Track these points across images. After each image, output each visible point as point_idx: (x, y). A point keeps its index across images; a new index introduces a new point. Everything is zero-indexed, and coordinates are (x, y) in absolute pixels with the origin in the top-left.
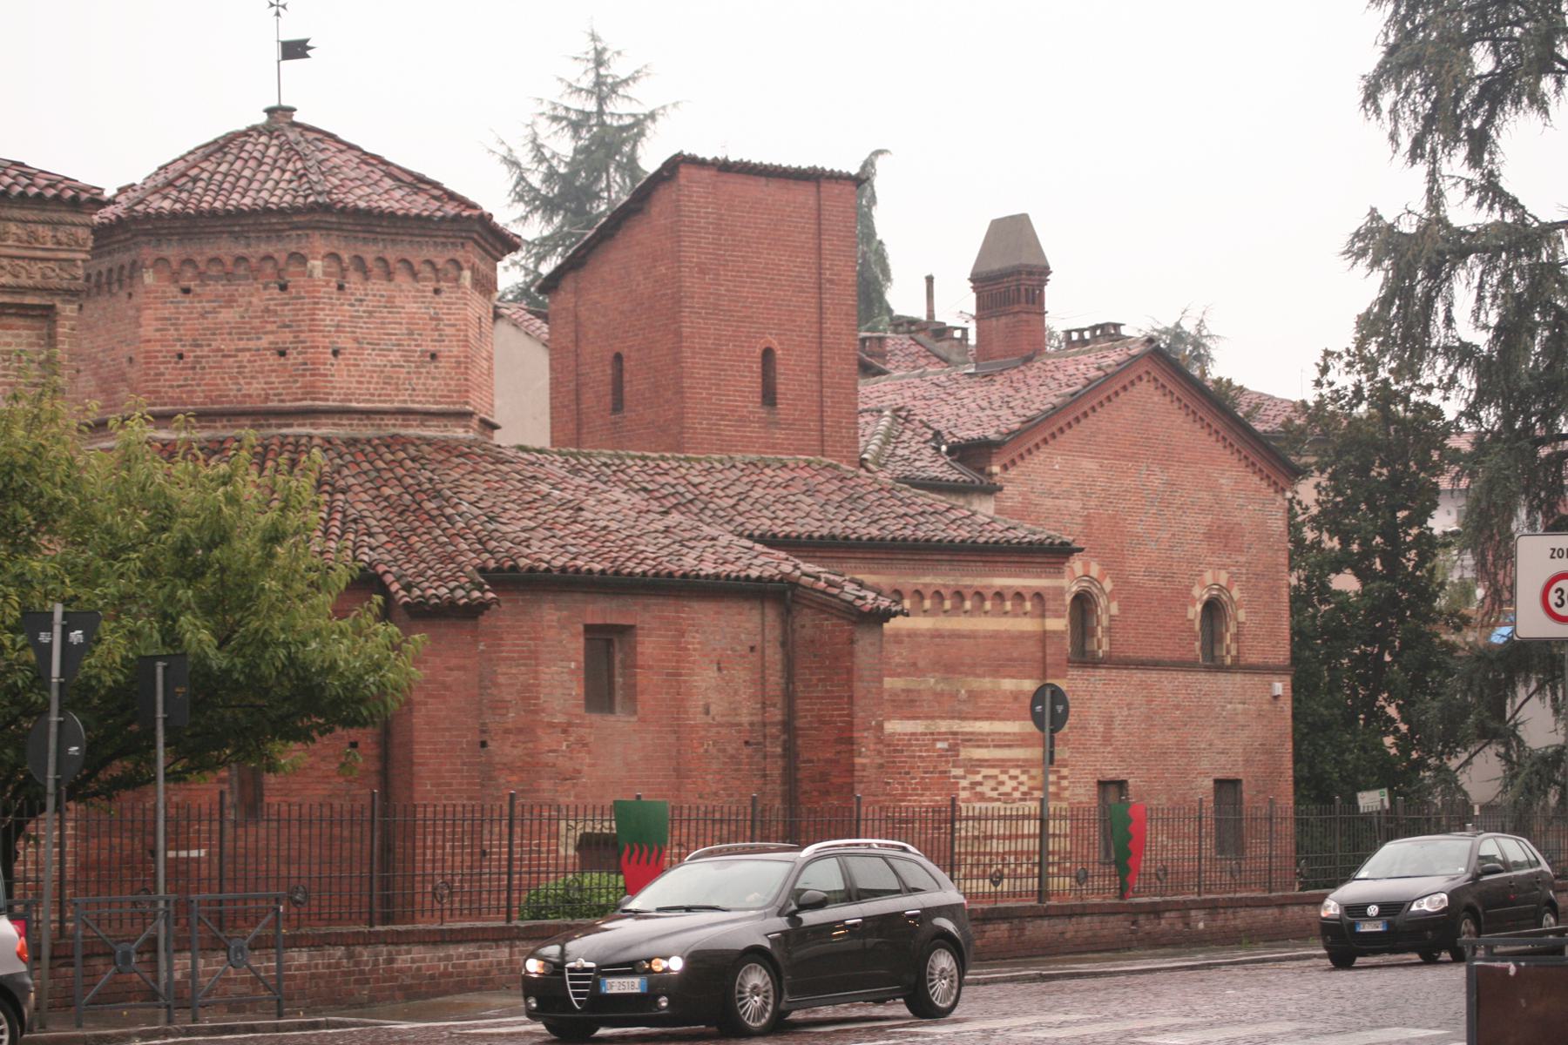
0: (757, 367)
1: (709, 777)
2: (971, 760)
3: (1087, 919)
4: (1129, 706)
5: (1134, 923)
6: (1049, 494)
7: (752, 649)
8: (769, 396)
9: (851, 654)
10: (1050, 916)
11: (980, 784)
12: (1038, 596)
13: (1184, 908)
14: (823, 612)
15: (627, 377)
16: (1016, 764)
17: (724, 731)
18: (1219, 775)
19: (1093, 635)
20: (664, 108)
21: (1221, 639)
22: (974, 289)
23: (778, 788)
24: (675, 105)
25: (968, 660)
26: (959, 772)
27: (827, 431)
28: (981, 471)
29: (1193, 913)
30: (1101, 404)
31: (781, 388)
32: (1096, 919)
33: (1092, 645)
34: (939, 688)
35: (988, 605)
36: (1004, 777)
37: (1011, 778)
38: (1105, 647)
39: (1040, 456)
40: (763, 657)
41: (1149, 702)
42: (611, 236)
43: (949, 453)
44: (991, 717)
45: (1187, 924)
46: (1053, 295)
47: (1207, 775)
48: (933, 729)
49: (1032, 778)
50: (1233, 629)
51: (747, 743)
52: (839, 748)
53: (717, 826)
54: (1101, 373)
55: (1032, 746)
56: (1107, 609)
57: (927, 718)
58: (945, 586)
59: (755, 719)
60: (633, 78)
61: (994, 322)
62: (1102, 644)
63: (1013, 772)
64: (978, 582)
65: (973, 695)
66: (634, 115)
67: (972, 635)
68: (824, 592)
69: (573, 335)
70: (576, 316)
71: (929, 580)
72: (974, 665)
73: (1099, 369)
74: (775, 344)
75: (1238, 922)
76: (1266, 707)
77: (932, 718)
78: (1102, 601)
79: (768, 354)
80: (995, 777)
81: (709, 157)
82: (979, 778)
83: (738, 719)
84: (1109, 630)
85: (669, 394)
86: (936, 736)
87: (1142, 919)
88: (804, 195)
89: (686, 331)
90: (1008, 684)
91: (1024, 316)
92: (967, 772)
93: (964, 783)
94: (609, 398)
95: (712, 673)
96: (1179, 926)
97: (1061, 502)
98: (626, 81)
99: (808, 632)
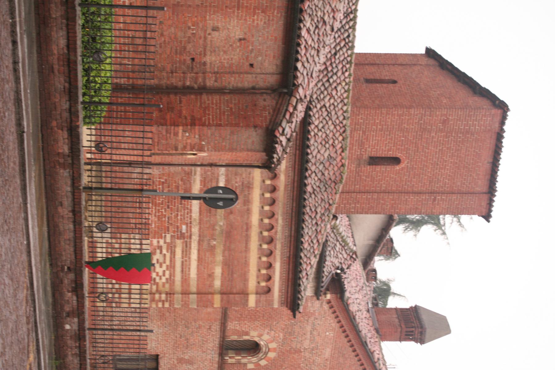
0: (391, 154)
1: (173, 29)
2: (175, 247)
3: (71, 226)
5: (69, 268)
6: (314, 329)
7: (252, 65)
8: (374, 161)
9: (247, 126)
10: (73, 193)
11: (161, 253)
12: (269, 290)
13: (79, 312)
14: (274, 111)
15: (385, 85)
16: (172, 275)
17: (201, 42)
19: (237, 354)
20: (447, 239)
22: (411, 307)
23: (164, 82)
24: (448, 243)
25: (233, 246)
26: (168, 240)
27: (354, 195)
28: (327, 289)
29: (76, 320)
30: (360, 360)
31: (378, 168)
32: (72, 234)
33: (231, 353)
34: (217, 228)
35: (264, 259)
36: (164, 267)
37: (164, 271)
38: (230, 361)
39: (334, 325)
40: (247, 73)
42: (459, 81)
43: (336, 273)
44: (200, 260)
45: (68, 315)
46: (410, 346)
48: (194, 223)
49: (164, 284)
51: (193, 59)
52: (189, 118)
53: (141, 34)
54: (376, 360)
55: (182, 286)
56: (251, 362)
57: (200, 220)
58: (276, 232)
59: (208, 66)
60: (461, 225)
61: (395, 316)
62: (231, 359)
63: (167, 273)
64: (278, 253)
65: (212, 249)
66: (444, 225)
67: (247, 249)
68: (287, 110)
69: (405, 63)
70: (414, 65)
71: (280, 222)
72: (230, 250)
73: (378, 359)
74: (402, 165)
75: (70, 358)
77: (200, 223)
78: (254, 359)
79: (396, 161)
80: (165, 262)
81: (505, 127)
82: (164, 251)
83: (208, 53)
84: (239, 363)
85: (377, 102)
86: (189, 225)
87: (72, 276)
88: (482, 185)
89: (412, 111)
90: (218, 271)
91: (399, 330)
92: (168, 244)
93: (162, 242)
94: (372, 78)
95: (238, 34)
96: (67, 308)
97: (308, 336)
98: (459, 222)
99: (261, 103)
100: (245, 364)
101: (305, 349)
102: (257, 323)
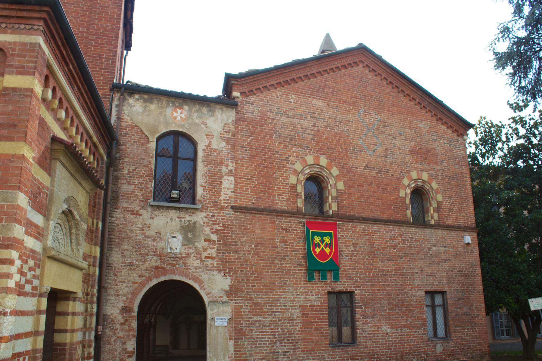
4: (355, 245)
6: (285, 114)
18: (428, 289)
21: (428, 211)
33: (326, 208)
38: (335, 207)
41: (371, 243)
47: (419, 288)
56: (336, 185)
76: (461, 249)
78: (332, 181)
100: (338, 191)
101: (314, 125)
102: (277, 174)
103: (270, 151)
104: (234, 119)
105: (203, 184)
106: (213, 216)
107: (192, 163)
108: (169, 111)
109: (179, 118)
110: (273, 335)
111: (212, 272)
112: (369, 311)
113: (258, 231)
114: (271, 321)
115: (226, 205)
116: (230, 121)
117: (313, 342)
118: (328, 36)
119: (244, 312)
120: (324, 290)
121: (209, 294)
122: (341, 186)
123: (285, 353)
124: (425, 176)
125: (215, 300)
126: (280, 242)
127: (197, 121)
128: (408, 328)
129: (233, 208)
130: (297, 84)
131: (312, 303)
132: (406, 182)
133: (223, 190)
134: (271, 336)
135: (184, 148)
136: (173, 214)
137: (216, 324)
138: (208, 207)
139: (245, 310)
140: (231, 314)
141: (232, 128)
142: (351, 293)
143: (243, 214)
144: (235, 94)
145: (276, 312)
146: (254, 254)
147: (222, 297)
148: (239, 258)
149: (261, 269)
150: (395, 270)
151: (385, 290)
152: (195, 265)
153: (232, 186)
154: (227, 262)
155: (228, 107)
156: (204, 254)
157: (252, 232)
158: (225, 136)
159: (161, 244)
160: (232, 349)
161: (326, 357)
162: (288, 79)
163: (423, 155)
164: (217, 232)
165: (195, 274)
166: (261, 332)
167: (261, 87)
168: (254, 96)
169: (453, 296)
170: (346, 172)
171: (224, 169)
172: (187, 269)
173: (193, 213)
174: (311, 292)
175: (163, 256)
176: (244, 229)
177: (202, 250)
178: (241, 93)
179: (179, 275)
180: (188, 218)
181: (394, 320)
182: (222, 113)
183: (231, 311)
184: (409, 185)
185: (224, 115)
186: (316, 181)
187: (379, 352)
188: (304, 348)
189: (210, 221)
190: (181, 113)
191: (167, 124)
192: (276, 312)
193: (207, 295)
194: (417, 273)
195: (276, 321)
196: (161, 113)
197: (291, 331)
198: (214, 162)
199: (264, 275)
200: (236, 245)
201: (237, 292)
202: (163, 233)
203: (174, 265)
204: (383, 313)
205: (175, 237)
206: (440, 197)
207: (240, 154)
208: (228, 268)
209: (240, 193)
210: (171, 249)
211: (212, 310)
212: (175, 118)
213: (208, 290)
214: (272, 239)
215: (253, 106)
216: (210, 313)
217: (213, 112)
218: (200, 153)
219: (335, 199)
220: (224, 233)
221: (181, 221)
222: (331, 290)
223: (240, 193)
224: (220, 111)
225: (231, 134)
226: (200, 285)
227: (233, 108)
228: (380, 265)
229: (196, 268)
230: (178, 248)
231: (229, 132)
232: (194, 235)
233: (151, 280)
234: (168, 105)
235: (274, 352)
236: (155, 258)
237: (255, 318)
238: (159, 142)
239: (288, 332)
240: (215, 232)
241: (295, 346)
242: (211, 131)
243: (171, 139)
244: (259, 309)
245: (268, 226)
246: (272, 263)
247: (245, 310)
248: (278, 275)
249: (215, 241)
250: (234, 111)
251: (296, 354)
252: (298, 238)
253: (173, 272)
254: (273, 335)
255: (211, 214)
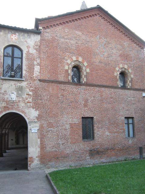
4: (94, 97)
6: (63, 37)
18: (126, 116)
33: (81, 80)
38: (85, 80)
39: (60, 27)
41: (101, 96)
47: (122, 116)
50: (130, 79)
76: (141, 99)
78: (84, 68)
101: (76, 43)
102: (59, 65)
103: (56, 54)
104: (40, 40)
105: (26, 69)
106: (30, 84)
107: (21, 59)
108: (9, 35)
109: (14, 39)
110: (58, 136)
111: (30, 109)
112: (100, 126)
113: (51, 90)
114: (57, 130)
115: (36, 79)
116: (38, 40)
117: (75, 139)
118: (84, 1)
119: (45, 126)
120: (80, 116)
121: (29, 118)
122: (88, 70)
123: (63, 144)
124: (126, 67)
125: (32, 121)
126: (61, 95)
127: (22, 40)
128: (117, 133)
129: (39, 80)
130: (69, 24)
131: (75, 122)
132: (117, 69)
133: (35, 72)
134: (57, 137)
135: (17, 53)
136: (12, 83)
137: (32, 132)
138: (28, 79)
139: (45, 125)
140: (39, 127)
141: (39, 44)
142: (92, 118)
143: (44, 83)
144: (40, 28)
145: (59, 126)
146: (49, 101)
147: (35, 120)
148: (42, 102)
149: (52, 107)
150: (112, 108)
151: (107, 117)
152: (22, 106)
153: (39, 70)
154: (37, 104)
155: (38, 34)
156: (27, 101)
157: (48, 91)
158: (36, 47)
159: (6, 97)
160: (39, 142)
161: (81, 146)
162: (65, 21)
163: (125, 57)
164: (32, 91)
165: (22, 110)
166: (52, 135)
167: (52, 25)
168: (49, 29)
169: (137, 119)
170: (90, 64)
171: (35, 63)
172: (19, 107)
173: (21, 82)
174: (75, 117)
175: (8, 102)
176: (44, 89)
177: (25, 99)
178: (43, 28)
179: (15, 110)
180: (19, 85)
181: (111, 130)
182: (34, 37)
183: (38, 126)
184: (118, 71)
185: (35, 38)
186: (77, 68)
187: (104, 144)
188: (71, 142)
189: (29, 86)
190: (15, 36)
191: (8, 41)
192: (59, 126)
193: (28, 119)
194: (121, 109)
195: (59, 130)
196: (5, 36)
197: (66, 134)
198: (31, 59)
199: (53, 110)
200: (41, 97)
201: (41, 117)
202: (7, 92)
203: (12, 106)
204: (106, 127)
205: (13, 93)
206: (132, 76)
207: (42, 56)
208: (37, 107)
209: (43, 73)
210: (11, 98)
211: (30, 125)
212: (12, 39)
213: (28, 117)
214: (57, 94)
215: (48, 34)
216: (29, 127)
217: (30, 36)
218: (24, 55)
219: (86, 76)
220: (36, 91)
221: (15, 86)
222: (83, 117)
223: (43, 73)
224: (33, 36)
225: (38, 46)
226: (25, 115)
227: (39, 34)
228: (105, 106)
229: (23, 107)
230: (15, 98)
231: (37, 46)
232: (21, 92)
233: (2, 112)
234: (9, 33)
235: (58, 144)
236: (4, 102)
237: (50, 129)
238: (5, 50)
239: (64, 135)
240: (31, 91)
241: (67, 141)
242: (29, 44)
243: (10, 49)
244: (51, 125)
245: (55, 88)
246: (57, 105)
247: (45, 125)
248: (60, 110)
249: (31, 95)
250: (40, 36)
251: (68, 144)
252: (69, 93)
253: (12, 109)
254: (58, 136)
255: (29, 83)
